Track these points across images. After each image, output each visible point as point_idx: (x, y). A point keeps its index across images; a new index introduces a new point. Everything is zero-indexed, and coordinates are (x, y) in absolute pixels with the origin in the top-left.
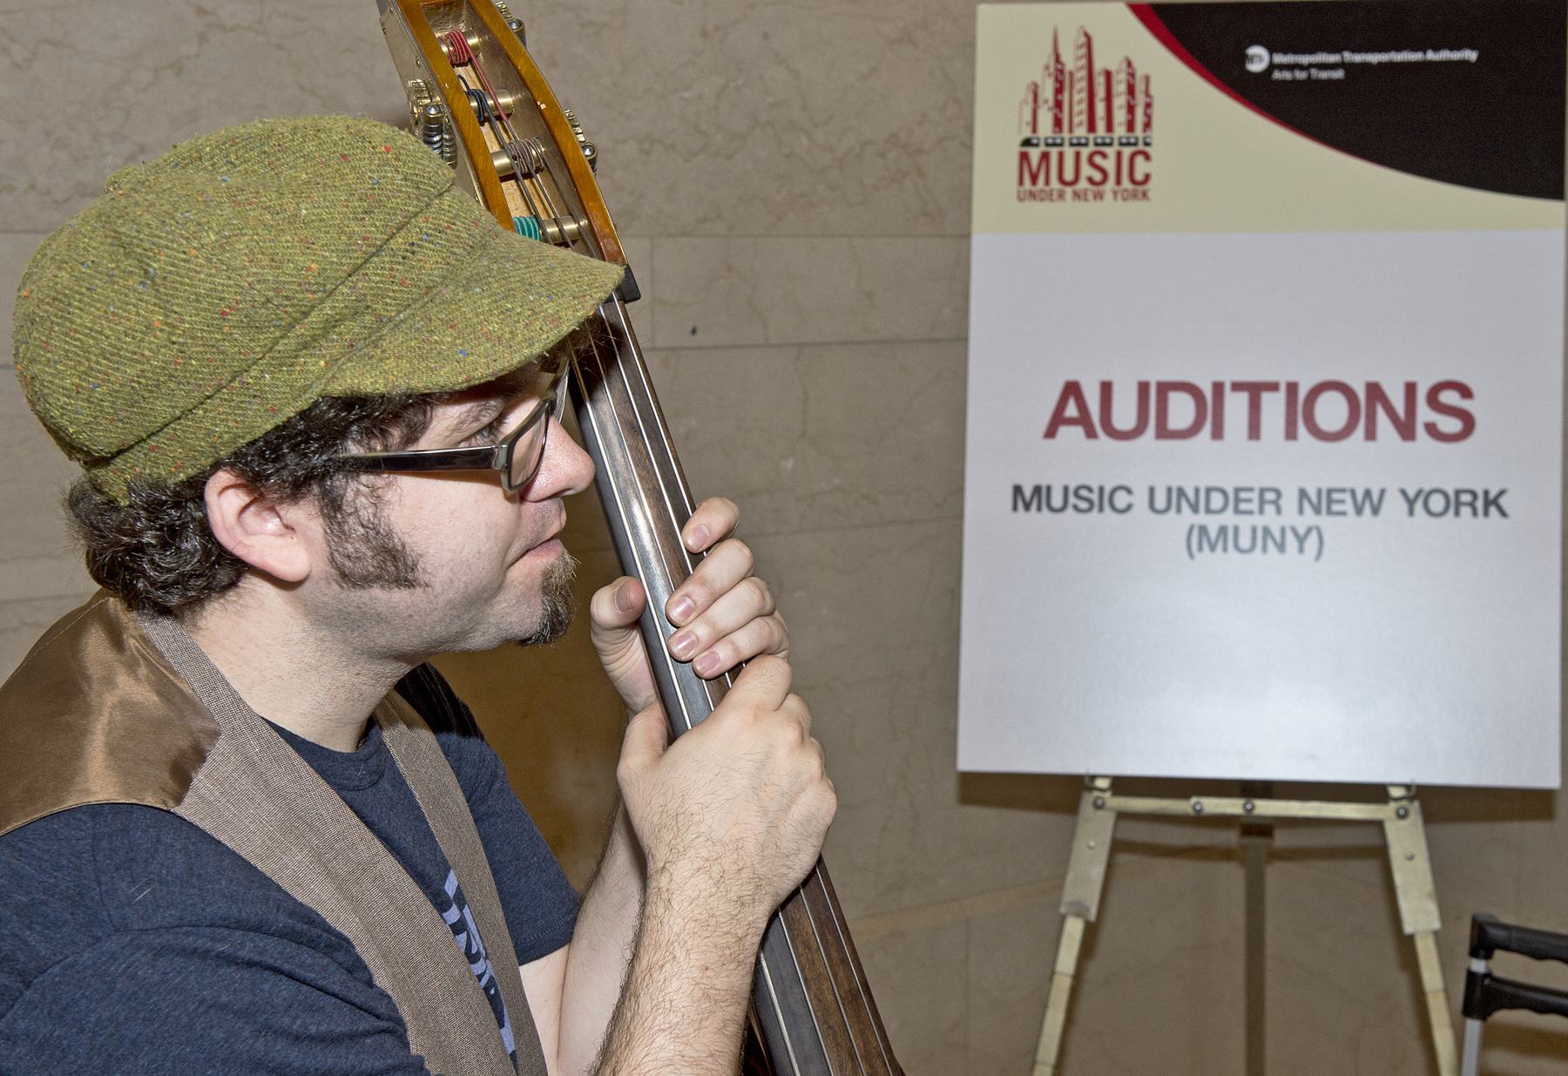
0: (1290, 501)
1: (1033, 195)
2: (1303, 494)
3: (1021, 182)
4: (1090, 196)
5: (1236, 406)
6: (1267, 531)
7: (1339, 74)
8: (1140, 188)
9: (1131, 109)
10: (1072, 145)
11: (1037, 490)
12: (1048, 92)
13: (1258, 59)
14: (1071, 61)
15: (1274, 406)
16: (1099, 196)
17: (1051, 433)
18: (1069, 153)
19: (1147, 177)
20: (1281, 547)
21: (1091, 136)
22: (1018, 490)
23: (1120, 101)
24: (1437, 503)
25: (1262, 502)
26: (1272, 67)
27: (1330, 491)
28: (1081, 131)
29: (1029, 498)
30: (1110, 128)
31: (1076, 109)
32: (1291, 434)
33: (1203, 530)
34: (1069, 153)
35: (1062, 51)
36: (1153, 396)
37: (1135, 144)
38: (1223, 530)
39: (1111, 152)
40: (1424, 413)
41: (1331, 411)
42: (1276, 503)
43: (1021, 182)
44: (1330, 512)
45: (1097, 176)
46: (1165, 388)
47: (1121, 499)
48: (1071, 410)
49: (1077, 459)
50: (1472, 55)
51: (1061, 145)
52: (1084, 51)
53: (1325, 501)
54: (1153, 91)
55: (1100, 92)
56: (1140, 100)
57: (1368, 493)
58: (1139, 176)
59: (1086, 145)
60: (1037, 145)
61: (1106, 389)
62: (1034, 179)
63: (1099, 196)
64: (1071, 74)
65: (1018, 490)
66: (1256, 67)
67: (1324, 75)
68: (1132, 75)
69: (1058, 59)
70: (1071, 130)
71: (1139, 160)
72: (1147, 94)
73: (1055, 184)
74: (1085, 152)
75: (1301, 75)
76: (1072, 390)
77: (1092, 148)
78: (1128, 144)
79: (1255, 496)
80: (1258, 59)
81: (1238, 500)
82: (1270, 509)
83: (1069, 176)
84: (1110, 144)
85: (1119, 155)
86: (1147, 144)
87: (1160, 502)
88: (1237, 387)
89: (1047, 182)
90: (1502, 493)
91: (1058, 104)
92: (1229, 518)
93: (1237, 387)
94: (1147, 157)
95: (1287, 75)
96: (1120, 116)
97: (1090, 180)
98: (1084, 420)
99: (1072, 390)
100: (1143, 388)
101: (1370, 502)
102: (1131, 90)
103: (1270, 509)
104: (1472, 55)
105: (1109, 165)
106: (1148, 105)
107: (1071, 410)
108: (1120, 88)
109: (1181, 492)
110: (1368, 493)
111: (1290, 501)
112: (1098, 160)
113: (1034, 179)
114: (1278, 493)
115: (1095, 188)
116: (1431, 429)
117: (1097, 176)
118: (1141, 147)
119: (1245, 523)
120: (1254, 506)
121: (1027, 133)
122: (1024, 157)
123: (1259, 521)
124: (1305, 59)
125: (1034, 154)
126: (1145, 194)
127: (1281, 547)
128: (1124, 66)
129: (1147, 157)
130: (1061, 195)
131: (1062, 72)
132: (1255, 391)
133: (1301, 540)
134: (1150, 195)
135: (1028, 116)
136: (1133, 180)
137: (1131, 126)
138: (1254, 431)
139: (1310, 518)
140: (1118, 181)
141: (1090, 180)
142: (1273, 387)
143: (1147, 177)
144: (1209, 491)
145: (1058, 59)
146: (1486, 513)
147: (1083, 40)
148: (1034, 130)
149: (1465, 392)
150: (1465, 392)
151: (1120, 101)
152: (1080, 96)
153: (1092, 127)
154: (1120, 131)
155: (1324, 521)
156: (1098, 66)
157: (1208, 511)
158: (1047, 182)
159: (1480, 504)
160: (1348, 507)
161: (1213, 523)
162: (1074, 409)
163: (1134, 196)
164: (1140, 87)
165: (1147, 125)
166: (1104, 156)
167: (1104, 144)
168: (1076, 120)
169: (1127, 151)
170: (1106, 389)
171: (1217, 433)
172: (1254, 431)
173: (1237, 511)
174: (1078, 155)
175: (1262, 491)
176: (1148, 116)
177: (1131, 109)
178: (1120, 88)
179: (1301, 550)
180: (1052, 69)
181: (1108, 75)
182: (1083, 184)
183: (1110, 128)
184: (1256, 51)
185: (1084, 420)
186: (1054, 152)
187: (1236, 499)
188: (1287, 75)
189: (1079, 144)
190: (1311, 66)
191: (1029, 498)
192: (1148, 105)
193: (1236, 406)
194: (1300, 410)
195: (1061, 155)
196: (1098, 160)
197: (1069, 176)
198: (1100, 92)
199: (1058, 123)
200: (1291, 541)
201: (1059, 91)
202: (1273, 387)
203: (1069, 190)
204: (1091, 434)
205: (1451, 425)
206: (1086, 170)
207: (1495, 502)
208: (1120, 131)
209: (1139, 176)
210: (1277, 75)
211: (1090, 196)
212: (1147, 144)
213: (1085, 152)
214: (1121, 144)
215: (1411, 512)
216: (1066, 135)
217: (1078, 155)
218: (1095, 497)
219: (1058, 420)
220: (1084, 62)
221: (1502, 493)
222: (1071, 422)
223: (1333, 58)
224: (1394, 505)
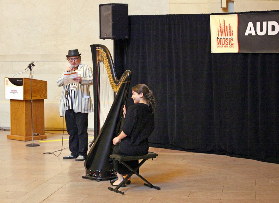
1: (219, 47)
14: (222, 25)
16: (227, 47)
19: (233, 43)
23: (228, 31)
28: (224, 36)
30: (228, 36)
37: (231, 38)
39: (228, 39)
45: (227, 44)
56: (231, 31)
58: (232, 44)
59: (225, 38)
62: (219, 45)
63: (227, 47)
68: (230, 27)
69: (220, 24)
71: (232, 40)
72: (232, 30)
73: (221, 45)
77: (226, 39)
83: (223, 44)
84: (228, 38)
85: (229, 40)
86: (233, 38)
89: (220, 45)
94: (233, 40)
96: (229, 33)
97: (226, 44)
105: (228, 41)
106: (232, 32)
108: (228, 29)
112: (227, 41)
113: (219, 45)
117: (227, 44)
118: (232, 39)
122: (217, 40)
129: (233, 40)
130: (222, 47)
131: (221, 26)
137: (230, 35)
140: (230, 44)
141: (226, 44)
143: (233, 43)
145: (220, 24)
147: (224, 21)
148: (218, 36)
151: (228, 31)
152: (223, 30)
156: (225, 26)
158: (220, 45)
165: (232, 35)
166: (227, 40)
169: (230, 39)
176: (232, 33)
178: (228, 29)
181: (227, 26)
182: (225, 45)
183: (228, 36)
186: (221, 39)
192: (232, 32)
195: (222, 40)
196: (227, 41)
197: (223, 44)
201: (221, 29)
203: (223, 46)
206: (226, 43)
208: (229, 36)
209: (232, 44)
212: (233, 38)
213: (225, 39)
217: (224, 40)
220: (224, 24)
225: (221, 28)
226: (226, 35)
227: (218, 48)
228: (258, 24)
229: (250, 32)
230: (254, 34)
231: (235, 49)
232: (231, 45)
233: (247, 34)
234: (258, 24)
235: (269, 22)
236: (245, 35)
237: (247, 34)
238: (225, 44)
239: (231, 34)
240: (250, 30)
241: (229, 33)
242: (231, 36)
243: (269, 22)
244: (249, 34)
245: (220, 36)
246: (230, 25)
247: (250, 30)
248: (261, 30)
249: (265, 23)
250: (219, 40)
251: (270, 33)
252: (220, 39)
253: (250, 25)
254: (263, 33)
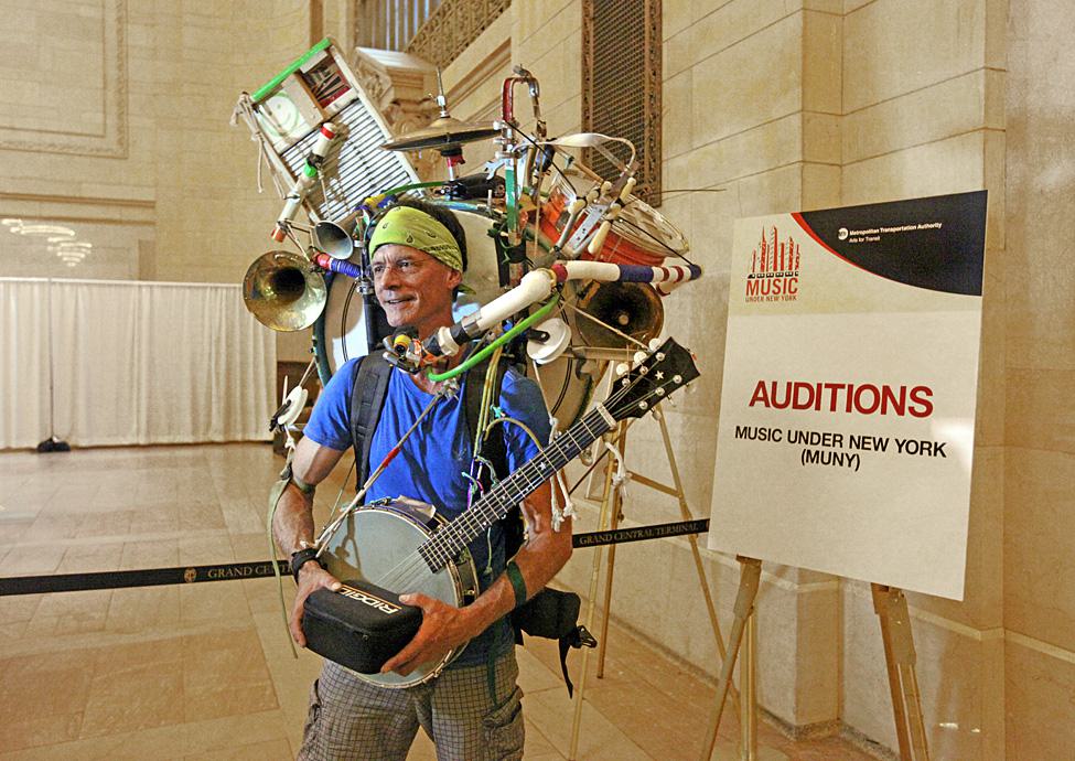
0: (846, 441)
2: (852, 438)
5: (826, 394)
6: (835, 454)
7: (878, 238)
9: (791, 260)
11: (745, 428)
12: (759, 255)
13: (844, 234)
15: (842, 395)
17: (752, 404)
18: (766, 280)
20: (841, 464)
22: (738, 428)
23: (787, 256)
24: (912, 447)
25: (835, 441)
26: (849, 237)
27: (864, 438)
28: (771, 271)
29: (742, 432)
30: (782, 269)
32: (849, 410)
33: (809, 452)
34: (766, 280)
36: (793, 389)
38: (817, 453)
40: (909, 402)
41: (867, 399)
42: (840, 441)
44: (863, 448)
45: (777, 290)
46: (798, 385)
47: (777, 435)
48: (761, 395)
49: (763, 417)
50: (939, 225)
53: (861, 443)
56: (795, 255)
57: (881, 440)
58: (793, 290)
61: (775, 384)
63: (776, 299)
65: (738, 428)
66: (842, 238)
67: (871, 239)
71: (793, 282)
74: (772, 279)
75: (861, 240)
76: (761, 385)
79: (831, 437)
80: (844, 234)
81: (824, 439)
82: (837, 444)
83: (765, 290)
85: (785, 280)
87: (792, 439)
88: (827, 386)
90: (943, 445)
91: (763, 259)
92: (820, 447)
93: (827, 386)
95: (856, 240)
96: (787, 263)
97: (774, 292)
98: (765, 399)
99: (761, 385)
100: (789, 384)
101: (881, 445)
102: (791, 251)
103: (837, 444)
104: (939, 225)
105: (781, 285)
107: (761, 395)
108: (787, 251)
109: (801, 433)
110: (881, 440)
111: (846, 441)
114: (841, 436)
116: (912, 410)
117: (777, 290)
119: (827, 450)
120: (831, 442)
122: (749, 283)
123: (833, 450)
124: (863, 233)
125: (753, 281)
127: (841, 464)
130: (762, 299)
132: (835, 387)
133: (850, 461)
136: (790, 292)
138: (833, 408)
139: (855, 450)
140: (784, 292)
141: (774, 292)
142: (842, 386)
144: (813, 434)
146: (935, 455)
149: (929, 393)
150: (929, 393)
151: (787, 256)
153: (775, 269)
154: (786, 270)
155: (860, 452)
156: (779, 243)
157: (812, 443)
159: (932, 449)
160: (872, 446)
161: (813, 449)
162: (763, 395)
164: (795, 250)
165: (797, 266)
169: (789, 278)
170: (775, 384)
171: (818, 408)
172: (833, 408)
173: (823, 444)
175: (835, 436)
177: (791, 260)
178: (787, 251)
179: (850, 465)
181: (783, 245)
184: (843, 230)
185: (765, 399)
186: (760, 280)
187: (823, 439)
188: (856, 240)
190: (866, 235)
191: (742, 432)
192: (798, 258)
193: (826, 394)
194: (853, 400)
197: (765, 290)
199: (762, 267)
200: (846, 461)
202: (842, 386)
204: (767, 405)
205: (921, 408)
206: (772, 288)
207: (940, 449)
208: (786, 270)
210: (851, 240)
213: (772, 279)
215: (900, 451)
218: (767, 434)
219: (755, 398)
221: (943, 445)
222: (760, 399)
223: (876, 231)
224: (892, 446)
225: (764, 250)
226: (779, 267)
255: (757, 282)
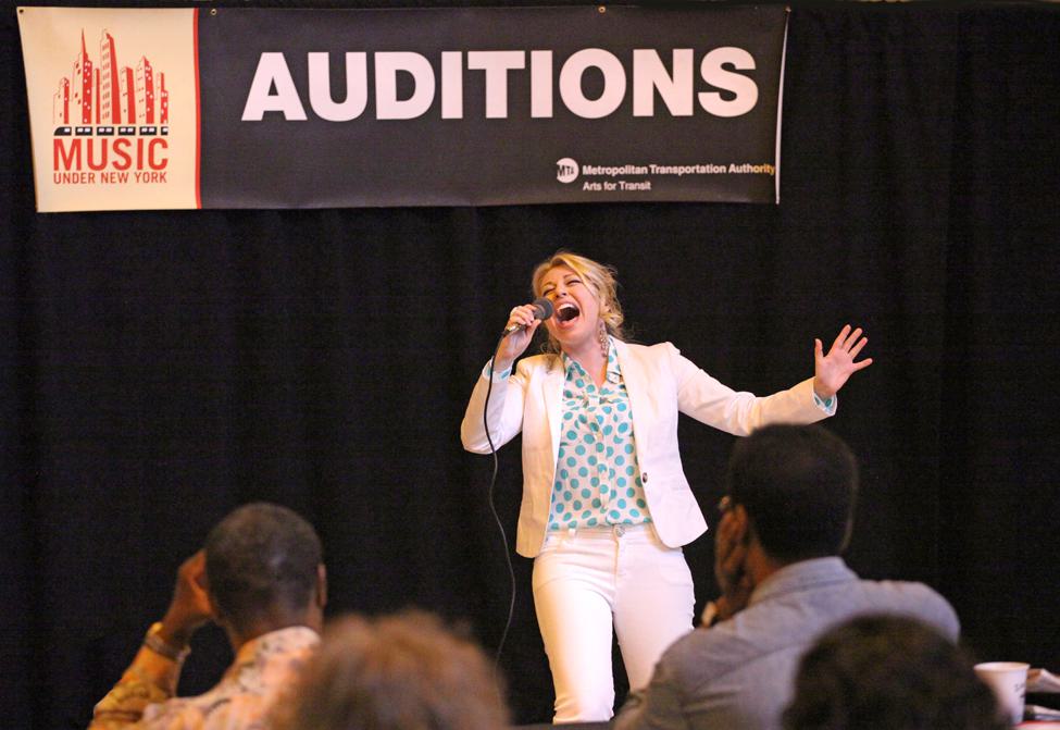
1: (67, 179)
3: (56, 167)
4: (116, 179)
8: (158, 171)
9: (150, 103)
10: (99, 134)
12: (77, 87)
14: (98, 60)
19: (165, 162)
21: (116, 127)
28: (107, 122)
30: (132, 119)
31: (102, 102)
34: (97, 140)
35: (87, 51)
37: (154, 133)
39: (133, 140)
43: (56, 167)
45: (122, 162)
51: (90, 133)
52: (108, 50)
54: (166, 88)
55: (123, 87)
58: (158, 162)
59: (112, 133)
60: (69, 134)
62: (68, 166)
64: (98, 71)
68: (150, 73)
70: (98, 121)
71: (158, 146)
72: (163, 90)
77: (116, 136)
78: (148, 133)
83: (97, 161)
84: (133, 133)
85: (140, 142)
86: (166, 134)
89: (79, 167)
91: (87, 98)
94: (165, 145)
96: (141, 109)
97: (116, 164)
105: (132, 151)
106: (164, 100)
108: (140, 84)
112: (122, 146)
113: (68, 166)
115: (121, 172)
117: (122, 162)
118: (159, 135)
121: (60, 123)
122: (58, 144)
125: (67, 141)
126: (162, 177)
128: (143, 64)
129: (165, 145)
130: (91, 179)
131: (90, 69)
134: (166, 177)
135: (61, 109)
137: (150, 118)
140: (140, 166)
141: (116, 164)
143: (165, 162)
147: (107, 41)
148: (66, 121)
151: (140, 95)
152: (106, 91)
153: (116, 119)
154: (141, 122)
156: (120, 66)
158: (79, 167)
163: (154, 178)
164: (157, 84)
165: (164, 117)
166: (128, 143)
167: (127, 133)
168: (102, 112)
169: (147, 139)
174: (104, 142)
176: (165, 110)
177: (150, 103)
178: (140, 84)
180: (81, 67)
181: (129, 72)
182: (110, 168)
183: (132, 119)
186: (84, 139)
189: (105, 133)
192: (164, 100)
195: (90, 143)
196: (122, 146)
197: (97, 161)
198: (123, 87)
199: (86, 114)
201: (87, 86)
203: (98, 174)
206: (112, 156)
208: (141, 122)
209: (158, 162)
211: (116, 179)
212: (166, 134)
213: (111, 140)
214: (142, 134)
216: (94, 125)
217: (104, 142)
220: (109, 60)
226: (124, 117)
227: (65, 187)
228: (319, 63)
229: (274, 104)
230: (295, 113)
231: (178, 191)
232: (151, 170)
233: (253, 111)
234: (319, 63)
235: (378, 55)
236: (247, 117)
237: (253, 111)
238: (110, 160)
239: (158, 112)
240: (273, 91)
241: (144, 103)
242: (157, 123)
243: (378, 55)
244: (266, 114)
245: (76, 120)
246: (147, 63)
247: (273, 91)
248: (339, 93)
249: (355, 62)
250: (67, 141)
251: (389, 108)
252: (73, 136)
253: (272, 66)
254: (352, 109)
255: (76, 144)
